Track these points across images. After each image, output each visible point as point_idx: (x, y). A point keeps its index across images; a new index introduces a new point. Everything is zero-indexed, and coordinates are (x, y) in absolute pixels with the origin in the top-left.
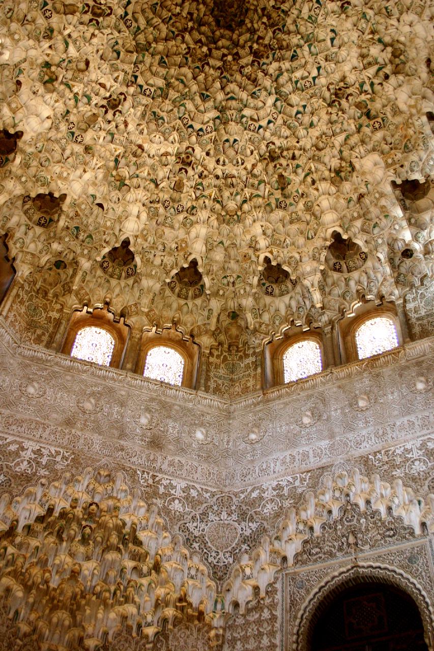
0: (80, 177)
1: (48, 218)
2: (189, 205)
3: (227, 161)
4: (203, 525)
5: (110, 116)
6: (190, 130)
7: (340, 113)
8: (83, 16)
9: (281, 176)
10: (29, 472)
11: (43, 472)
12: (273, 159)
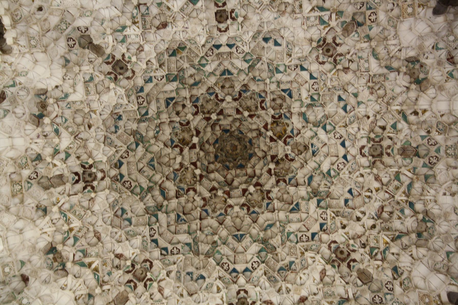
2: (389, 273)
3: (362, 209)
6: (316, 238)
7: (348, 57)
8: (137, 291)
9: (404, 152)
12: (381, 155)
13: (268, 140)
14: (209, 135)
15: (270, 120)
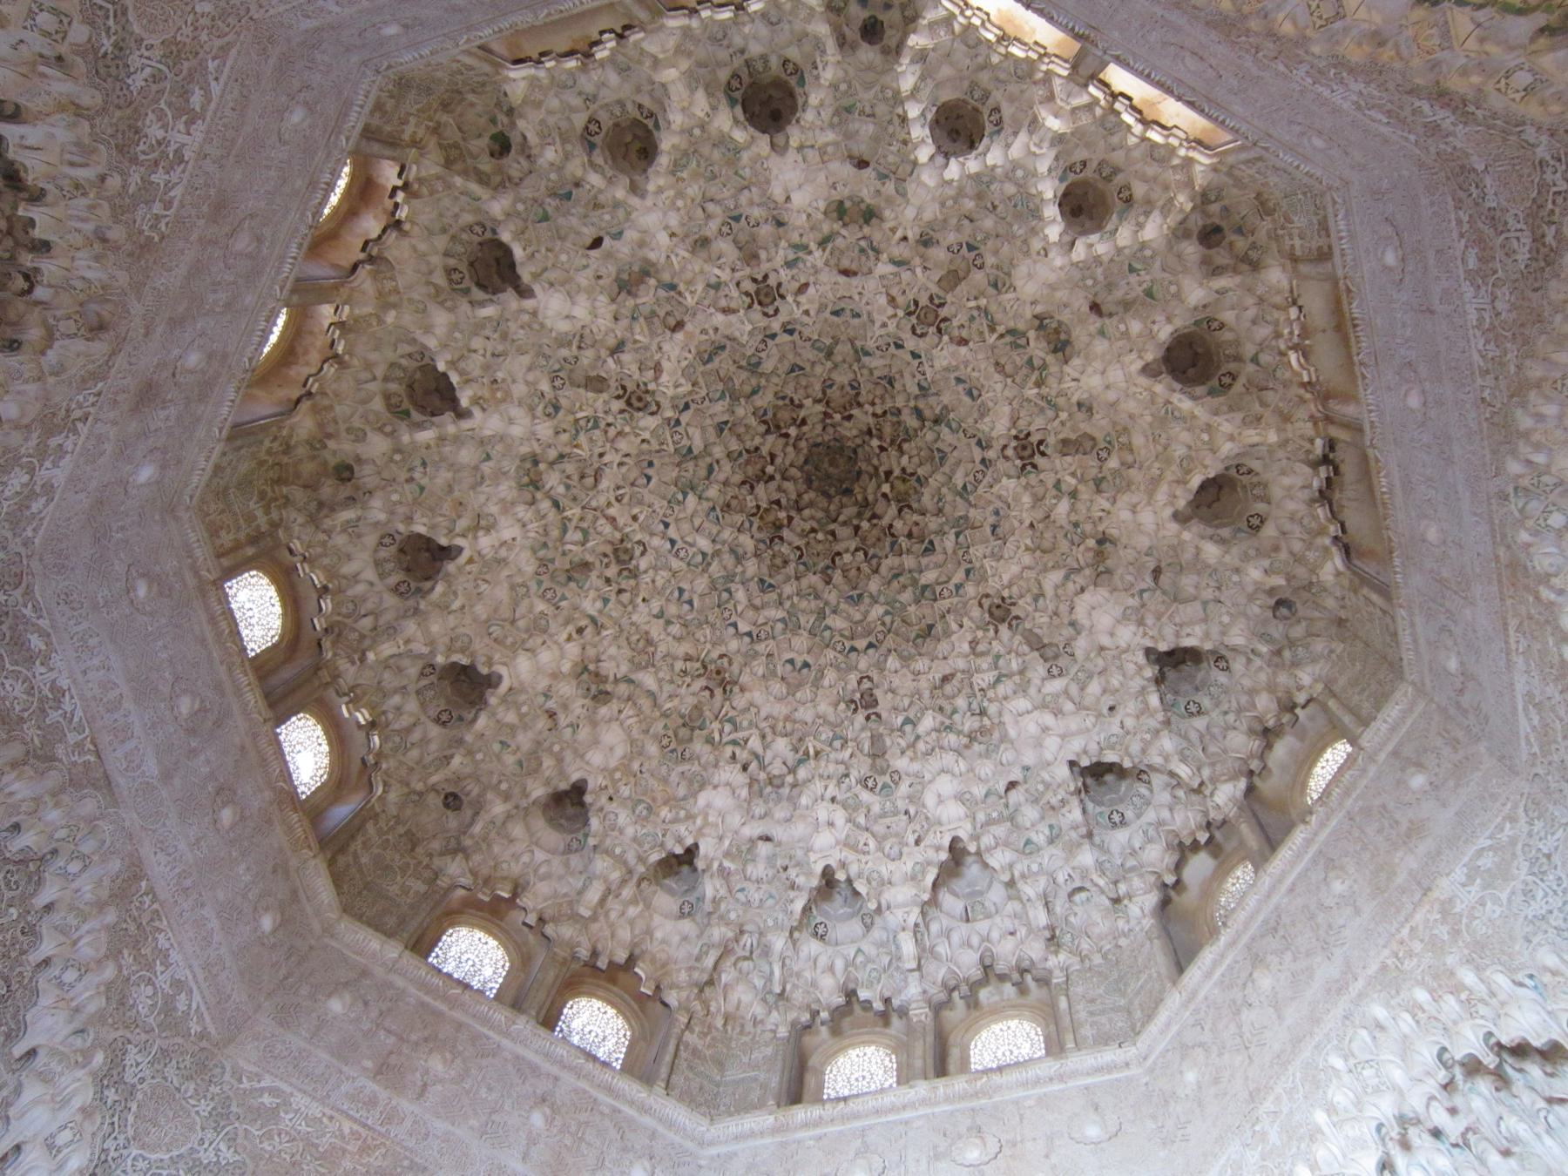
0: (666, 228)
1: (597, 140)
2: (563, 402)
3: (624, 469)
5: (749, 286)
9: (586, 566)
10: (142, 147)
11: (135, 179)
12: (616, 551)
13: (784, 501)
14: (870, 490)
15: (786, 533)
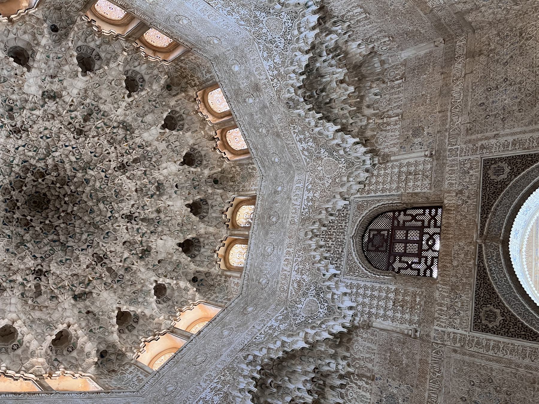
0: (173, 205)
3: (104, 150)
4: (277, 39)
5: (137, 214)
6: (108, 176)
7: (26, 123)
9: (85, 120)
11: (307, 134)
15: (33, 177)
